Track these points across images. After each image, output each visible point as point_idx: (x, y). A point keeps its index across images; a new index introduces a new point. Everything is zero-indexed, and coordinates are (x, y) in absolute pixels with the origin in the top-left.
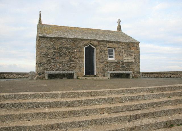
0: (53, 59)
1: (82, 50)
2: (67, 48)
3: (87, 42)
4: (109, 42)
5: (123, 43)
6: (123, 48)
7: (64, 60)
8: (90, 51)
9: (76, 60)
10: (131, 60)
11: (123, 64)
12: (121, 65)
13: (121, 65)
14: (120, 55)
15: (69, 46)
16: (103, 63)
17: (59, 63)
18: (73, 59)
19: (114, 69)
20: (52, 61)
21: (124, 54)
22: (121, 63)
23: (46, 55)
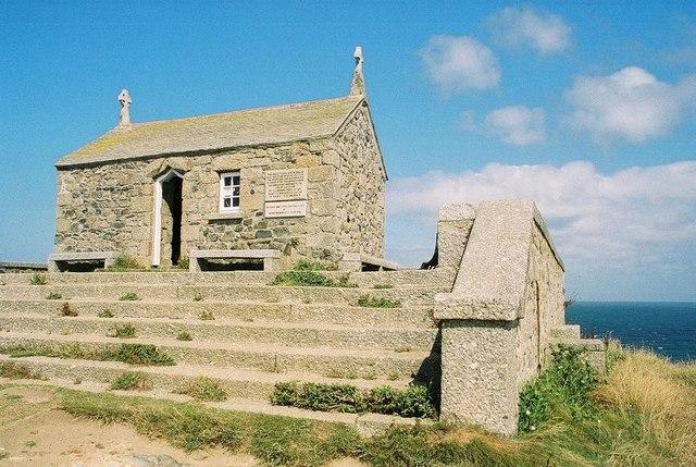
0: (83, 221)
1: (147, 190)
2: (112, 190)
3: (155, 165)
4: (218, 152)
5: (266, 146)
6: (266, 168)
7: (104, 224)
8: (173, 191)
9: (129, 222)
10: (293, 209)
11: (263, 224)
12: (256, 227)
13: (256, 227)
14: (253, 192)
15: (113, 183)
16: (198, 224)
17: (93, 231)
18: (123, 218)
19: (233, 244)
20: (81, 226)
21: (268, 188)
22: (257, 220)
23: (69, 213)
